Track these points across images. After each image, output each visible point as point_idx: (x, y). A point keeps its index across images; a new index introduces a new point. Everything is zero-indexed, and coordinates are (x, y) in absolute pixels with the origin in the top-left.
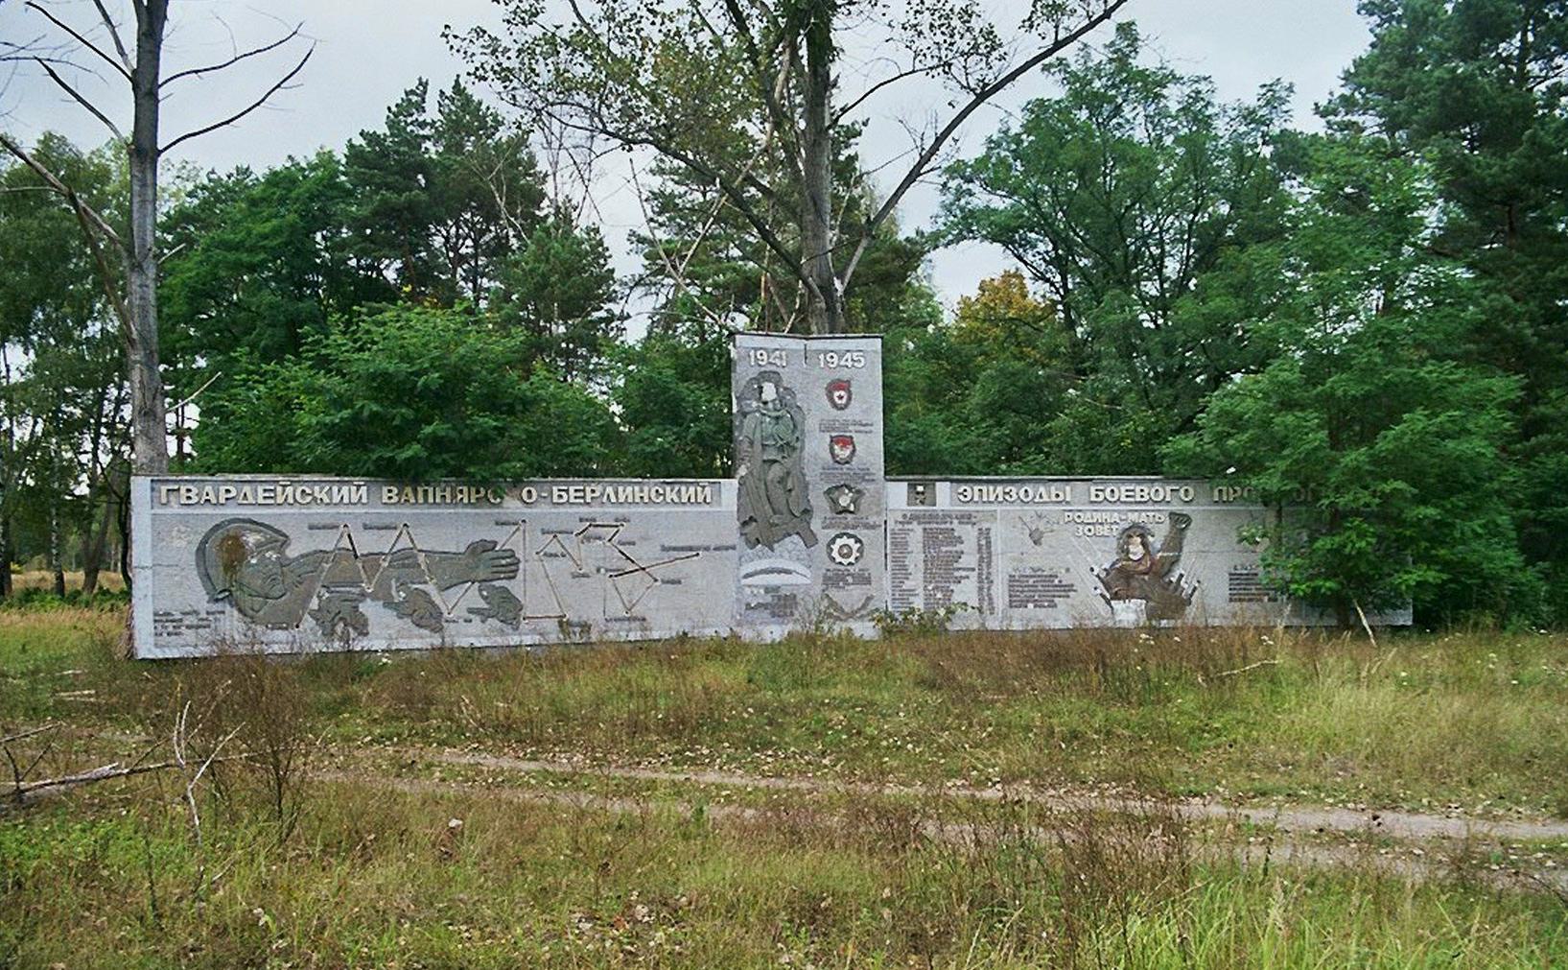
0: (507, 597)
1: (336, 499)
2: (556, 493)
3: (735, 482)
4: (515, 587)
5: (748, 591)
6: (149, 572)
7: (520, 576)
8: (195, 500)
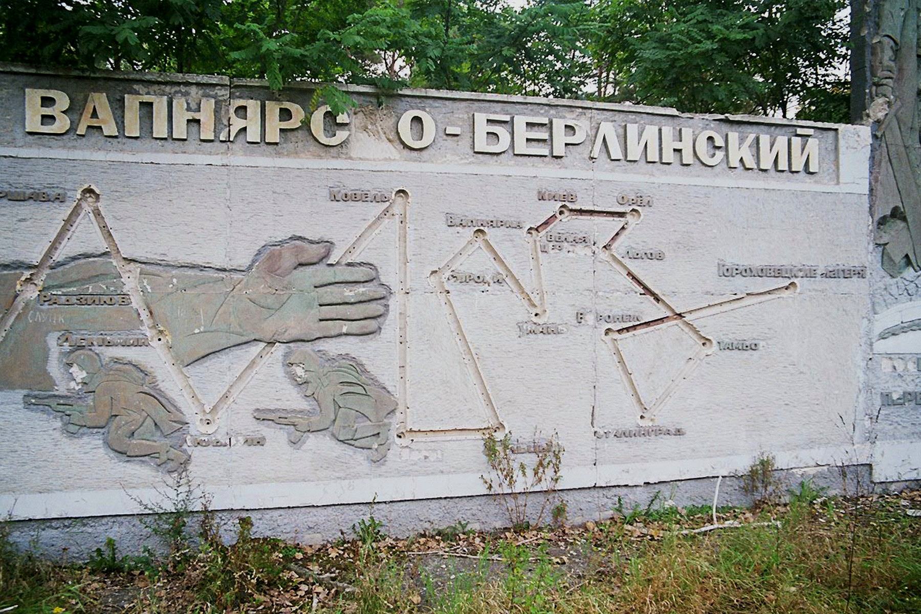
0: (357, 383)
2: (482, 128)
3: (864, 132)
4: (377, 356)
5: (886, 365)
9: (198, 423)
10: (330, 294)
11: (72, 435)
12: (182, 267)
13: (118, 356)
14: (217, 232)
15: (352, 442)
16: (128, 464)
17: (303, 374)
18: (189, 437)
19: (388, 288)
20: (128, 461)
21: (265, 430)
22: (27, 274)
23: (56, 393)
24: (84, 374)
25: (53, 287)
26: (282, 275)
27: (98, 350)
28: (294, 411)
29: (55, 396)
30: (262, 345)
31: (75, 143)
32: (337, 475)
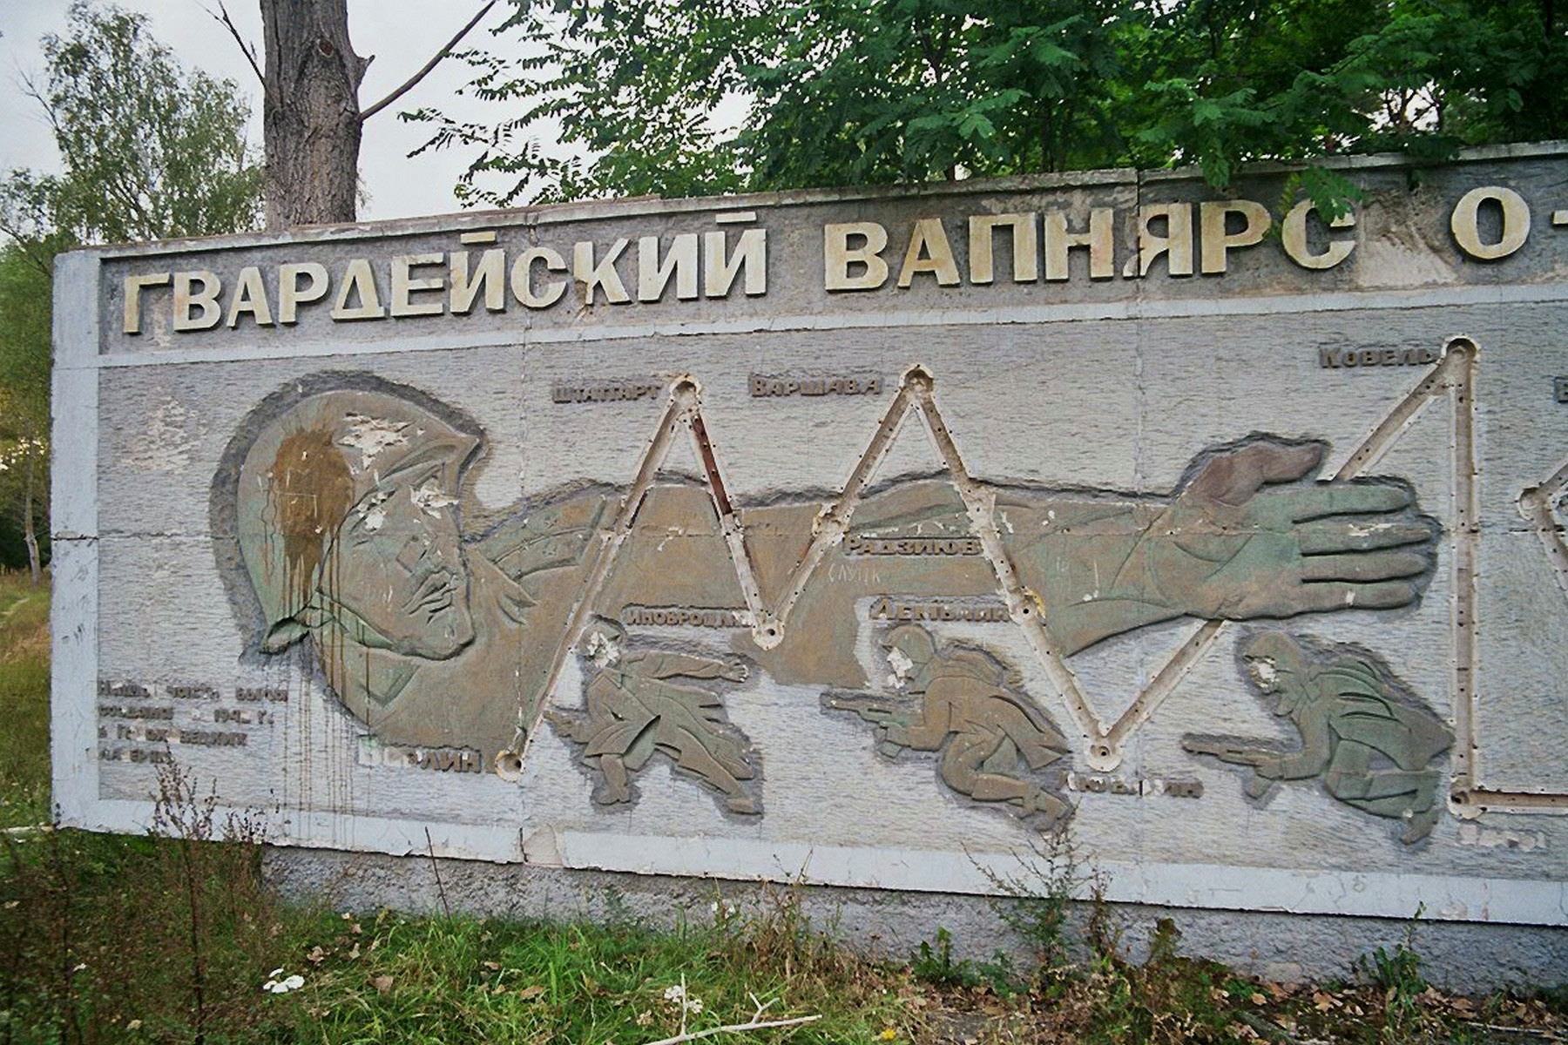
1: (650, 285)
6: (88, 553)
8: (207, 321)
9: (1087, 752)
11: (889, 759)
12: (1063, 490)
13: (960, 636)
14: (1121, 432)
15: (1358, 803)
16: (973, 813)
17: (1272, 676)
18: (1071, 775)
19: (1434, 522)
20: (973, 808)
21: (1201, 772)
22: (827, 507)
23: (867, 692)
24: (909, 665)
25: (864, 526)
27: (929, 625)
28: (1255, 741)
29: (866, 696)
30: (1199, 624)
31: (895, 301)
32: (1333, 861)
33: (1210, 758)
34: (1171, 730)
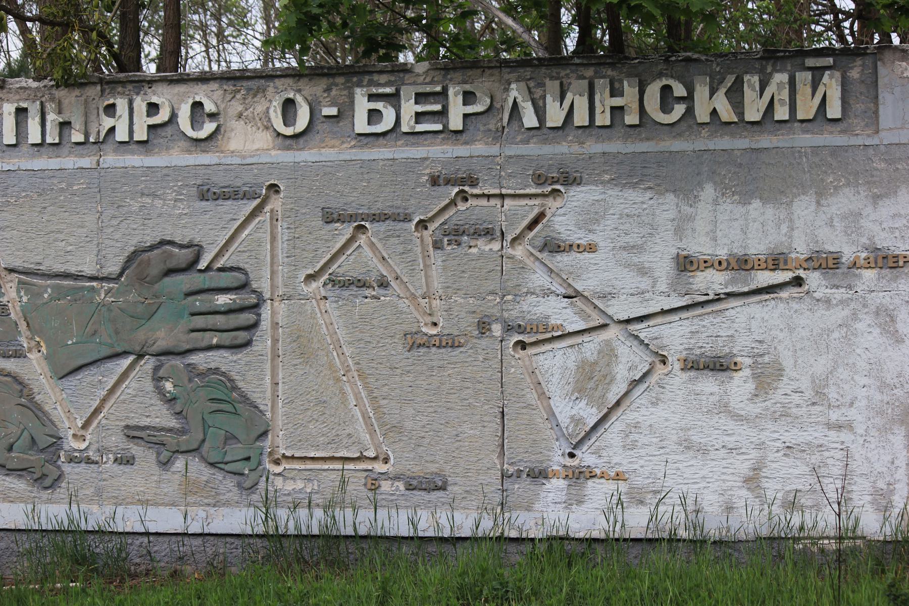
0: (228, 399)
2: (362, 105)
7: (263, 343)
9: (70, 438)
10: (198, 303)
14: (88, 239)
16: (7, 479)
17: (172, 389)
18: (62, 453)
19: (259, 294)
20: (7, 475)
21: (136, 450)
26: (152, 283)
30: (131, 358)
32: (206, 501)
33: (140, 440)
34: (118, 423)
